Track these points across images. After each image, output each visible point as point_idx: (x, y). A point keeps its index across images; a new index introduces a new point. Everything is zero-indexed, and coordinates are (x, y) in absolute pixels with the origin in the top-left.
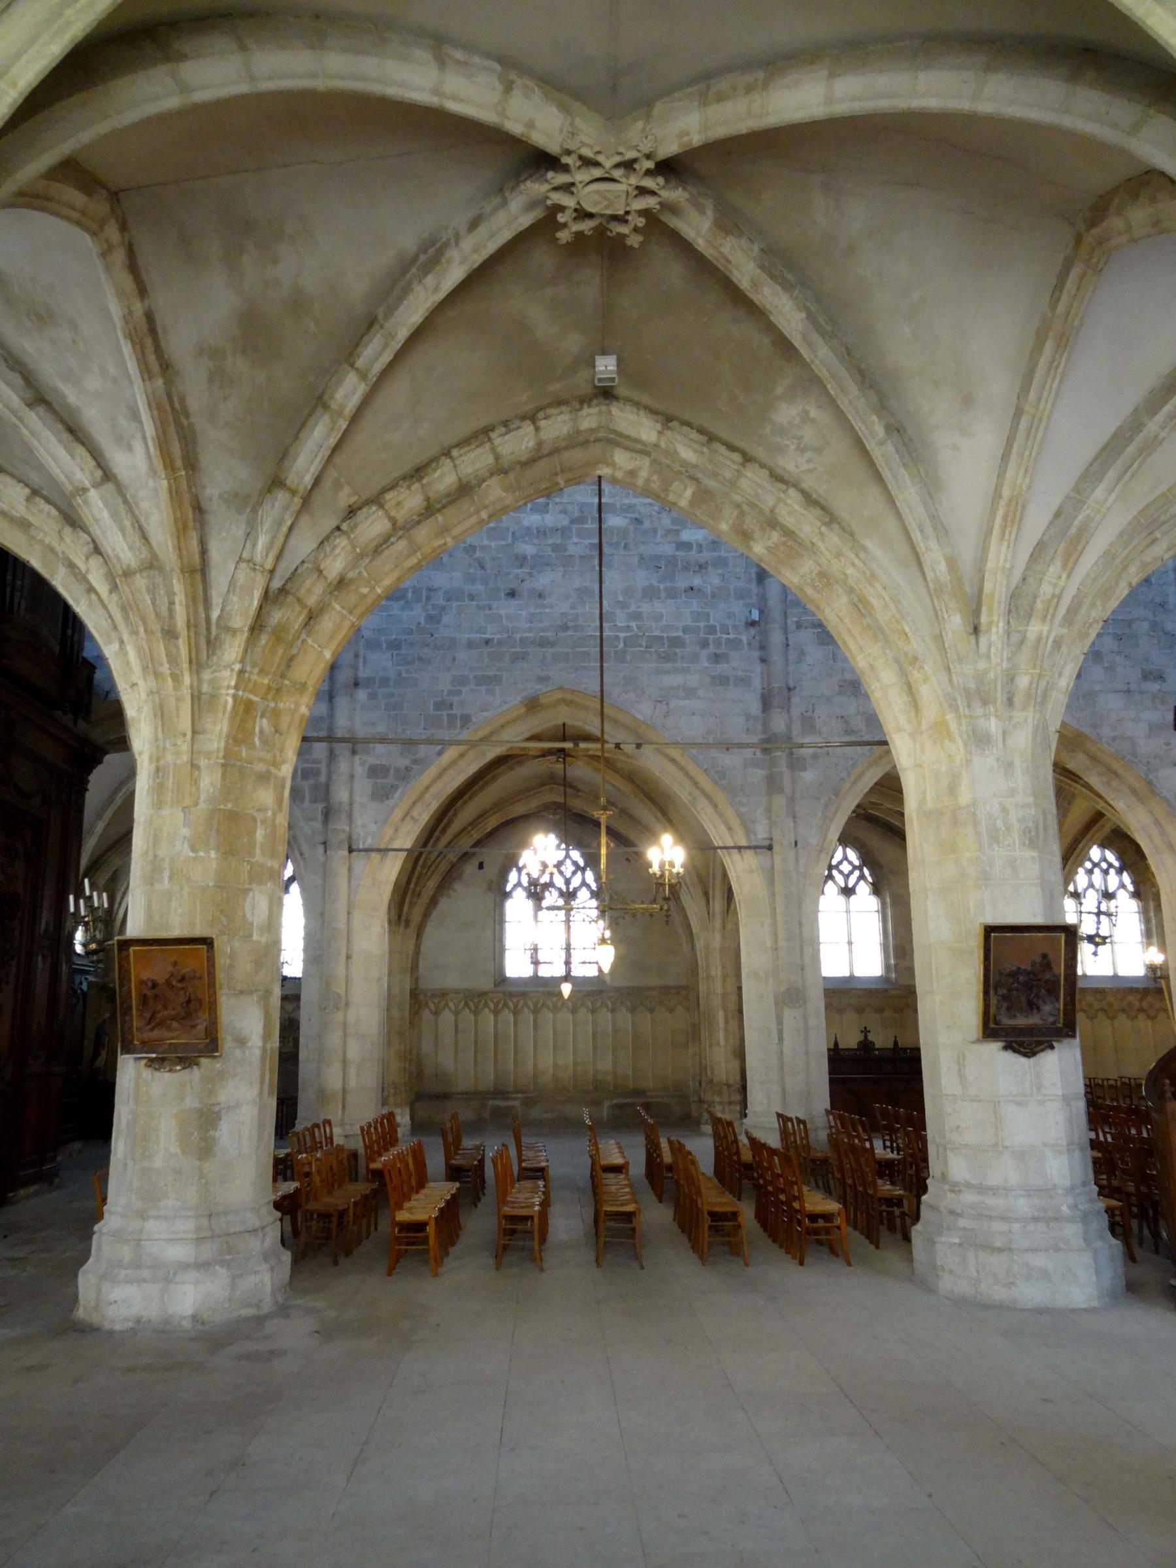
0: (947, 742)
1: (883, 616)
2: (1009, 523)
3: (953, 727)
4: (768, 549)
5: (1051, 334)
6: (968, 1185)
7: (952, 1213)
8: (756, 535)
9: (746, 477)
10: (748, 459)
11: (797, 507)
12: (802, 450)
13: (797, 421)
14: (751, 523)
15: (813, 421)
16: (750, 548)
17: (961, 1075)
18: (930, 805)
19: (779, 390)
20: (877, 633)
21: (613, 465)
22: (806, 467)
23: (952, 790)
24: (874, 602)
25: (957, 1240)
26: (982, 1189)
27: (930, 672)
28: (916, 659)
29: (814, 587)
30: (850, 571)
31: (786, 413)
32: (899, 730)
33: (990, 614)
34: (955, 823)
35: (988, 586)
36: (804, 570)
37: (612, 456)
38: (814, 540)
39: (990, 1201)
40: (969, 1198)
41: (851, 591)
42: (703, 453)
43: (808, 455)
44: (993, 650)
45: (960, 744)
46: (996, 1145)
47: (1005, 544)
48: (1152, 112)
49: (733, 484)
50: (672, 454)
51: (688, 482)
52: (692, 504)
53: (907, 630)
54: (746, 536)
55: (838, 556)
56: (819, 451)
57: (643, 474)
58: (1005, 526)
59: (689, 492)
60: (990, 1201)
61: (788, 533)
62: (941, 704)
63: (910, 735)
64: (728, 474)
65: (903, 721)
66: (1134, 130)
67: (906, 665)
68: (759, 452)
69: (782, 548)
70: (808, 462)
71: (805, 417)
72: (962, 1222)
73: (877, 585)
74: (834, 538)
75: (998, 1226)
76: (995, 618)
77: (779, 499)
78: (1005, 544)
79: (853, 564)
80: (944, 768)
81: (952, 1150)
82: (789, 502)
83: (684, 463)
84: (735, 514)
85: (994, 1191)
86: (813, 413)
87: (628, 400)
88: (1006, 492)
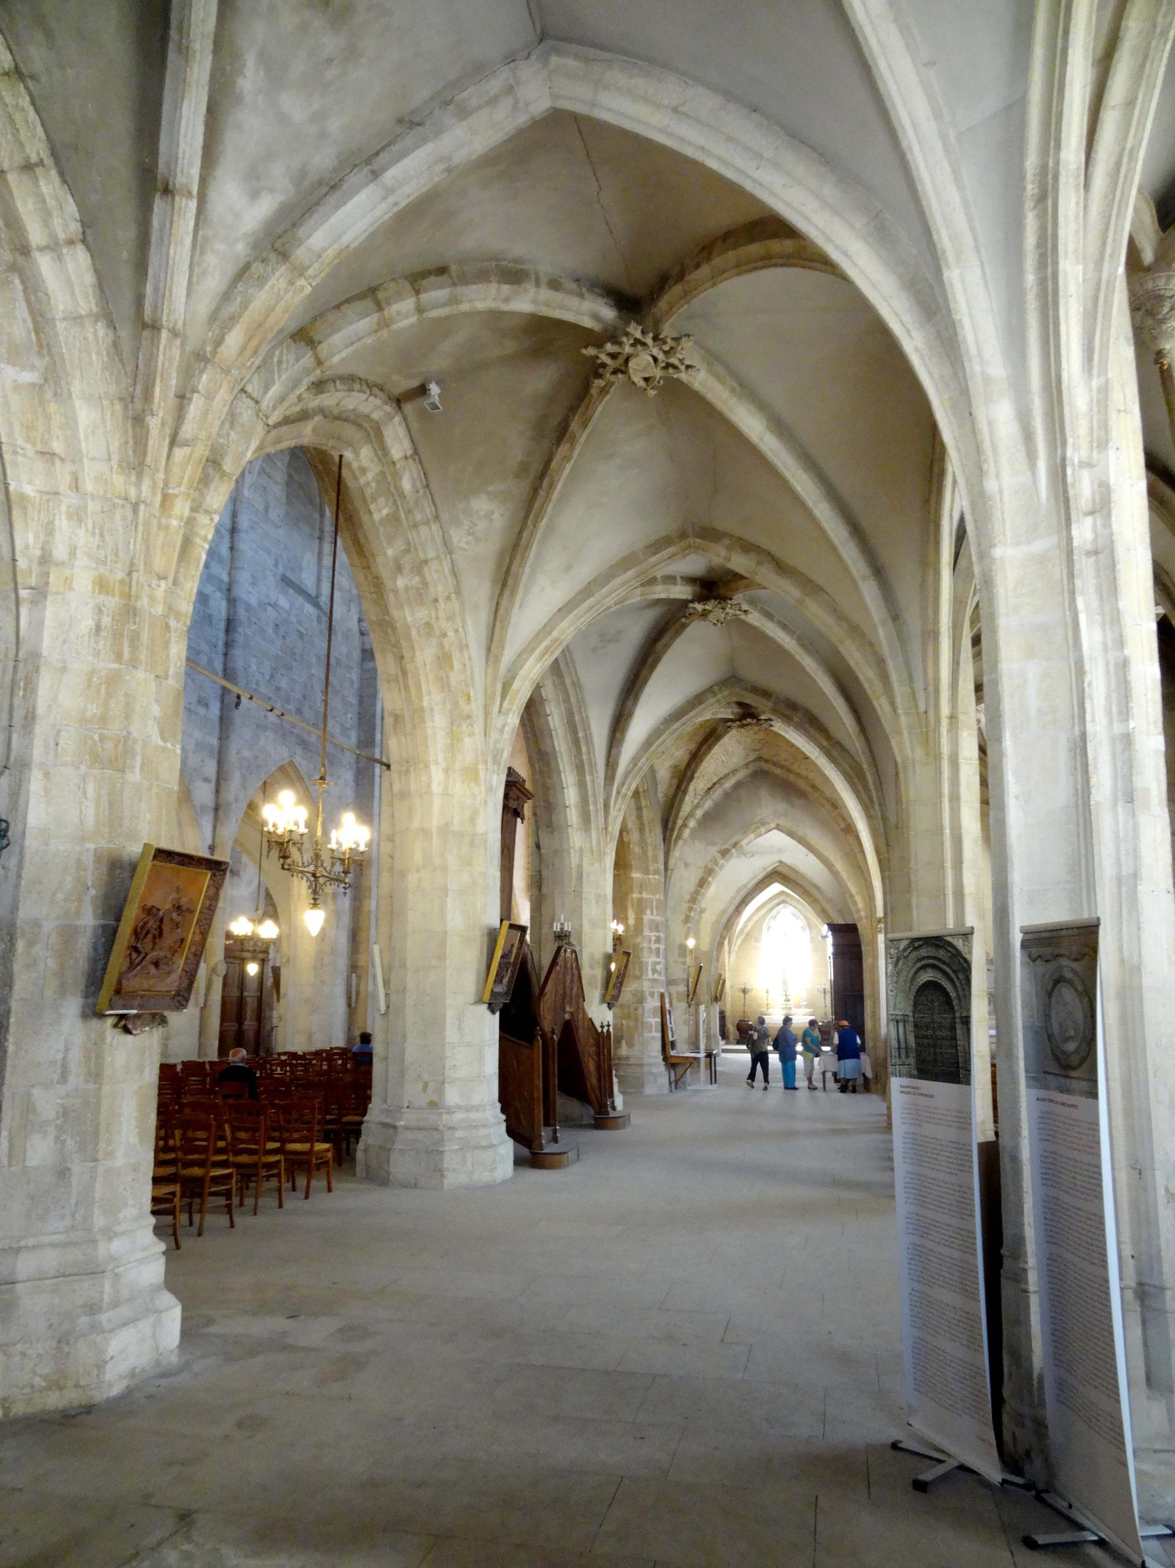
0: (472, 785)
1: (455, 677)
2: (549, 653)
3: (482, 775)
4: (406, 586)
5: (637, 568)
6: (459, 1107)
7: (450, 1128)
8: (405, 572)
9: (430, 528)
10: (437, 517)
11: (446, 570)
12: (469, 533)
13: (482, 514)
14: (407, 561)
15: (491, 520)
16: (395, 580)
17: (460, 1028)
18: (456, 826)
19: (491, 488)
20: (445, 685)
21: (357, 454)
22: (463, 545)
23: (473, 819)
24: (456, 665)
25: (456, 1147)
26: (468, 1109)
27: (477, 731)
28: (469, 717)
29: (419, 632)
30: (451, 634)
31: (481, 504)
32: (437, 763)
33: (511, 703)
34: (472, 845)
35: (516, 685)
36: (418, 615)
37: (361, 447)
38: (440, 600)
39: (474, 1116)
40: (459, 1116)
41: (441, 646)
42: (418, 492)
43: (470, 538)
44: (506, 728)
45: (483, 789)
46: (479, 1076)
47: (540, 664)
48: (872, 578)
49: (415, 526)
50: (397, 476)
51: (390, 504)
52: (382, 520)
53: (472, 695)
54: (399, 569)
55: (450, 618)
56: (478, 540)
57: (370, 476)
58: (545, 654)
59: (385, 512)
60: (474, 1116)
61: (425, 583)
62: (477, 756)
63: (443, 770)
64: (419, 517)
65: (441, 758)
66: (864, 578)
67: (458, 718)
68: (445, 516)
69: (414, 591)
70: (467, 543)
71: (488, 516)
72: (458, 1134)
73: (465, 653)
74: (456, 605)
75: (483, 1132)
76: (514, 708)
77: (438, 557)
78: (540, 664)
79: (457, 631)
80: (468, 802)
81: (449, 1083)
82: (444, 564)
83: (398, 488)
84: (403, 548)
85: (477, 1108)
86: (496, 516)
87: (405, 419)
88: (555, 633)
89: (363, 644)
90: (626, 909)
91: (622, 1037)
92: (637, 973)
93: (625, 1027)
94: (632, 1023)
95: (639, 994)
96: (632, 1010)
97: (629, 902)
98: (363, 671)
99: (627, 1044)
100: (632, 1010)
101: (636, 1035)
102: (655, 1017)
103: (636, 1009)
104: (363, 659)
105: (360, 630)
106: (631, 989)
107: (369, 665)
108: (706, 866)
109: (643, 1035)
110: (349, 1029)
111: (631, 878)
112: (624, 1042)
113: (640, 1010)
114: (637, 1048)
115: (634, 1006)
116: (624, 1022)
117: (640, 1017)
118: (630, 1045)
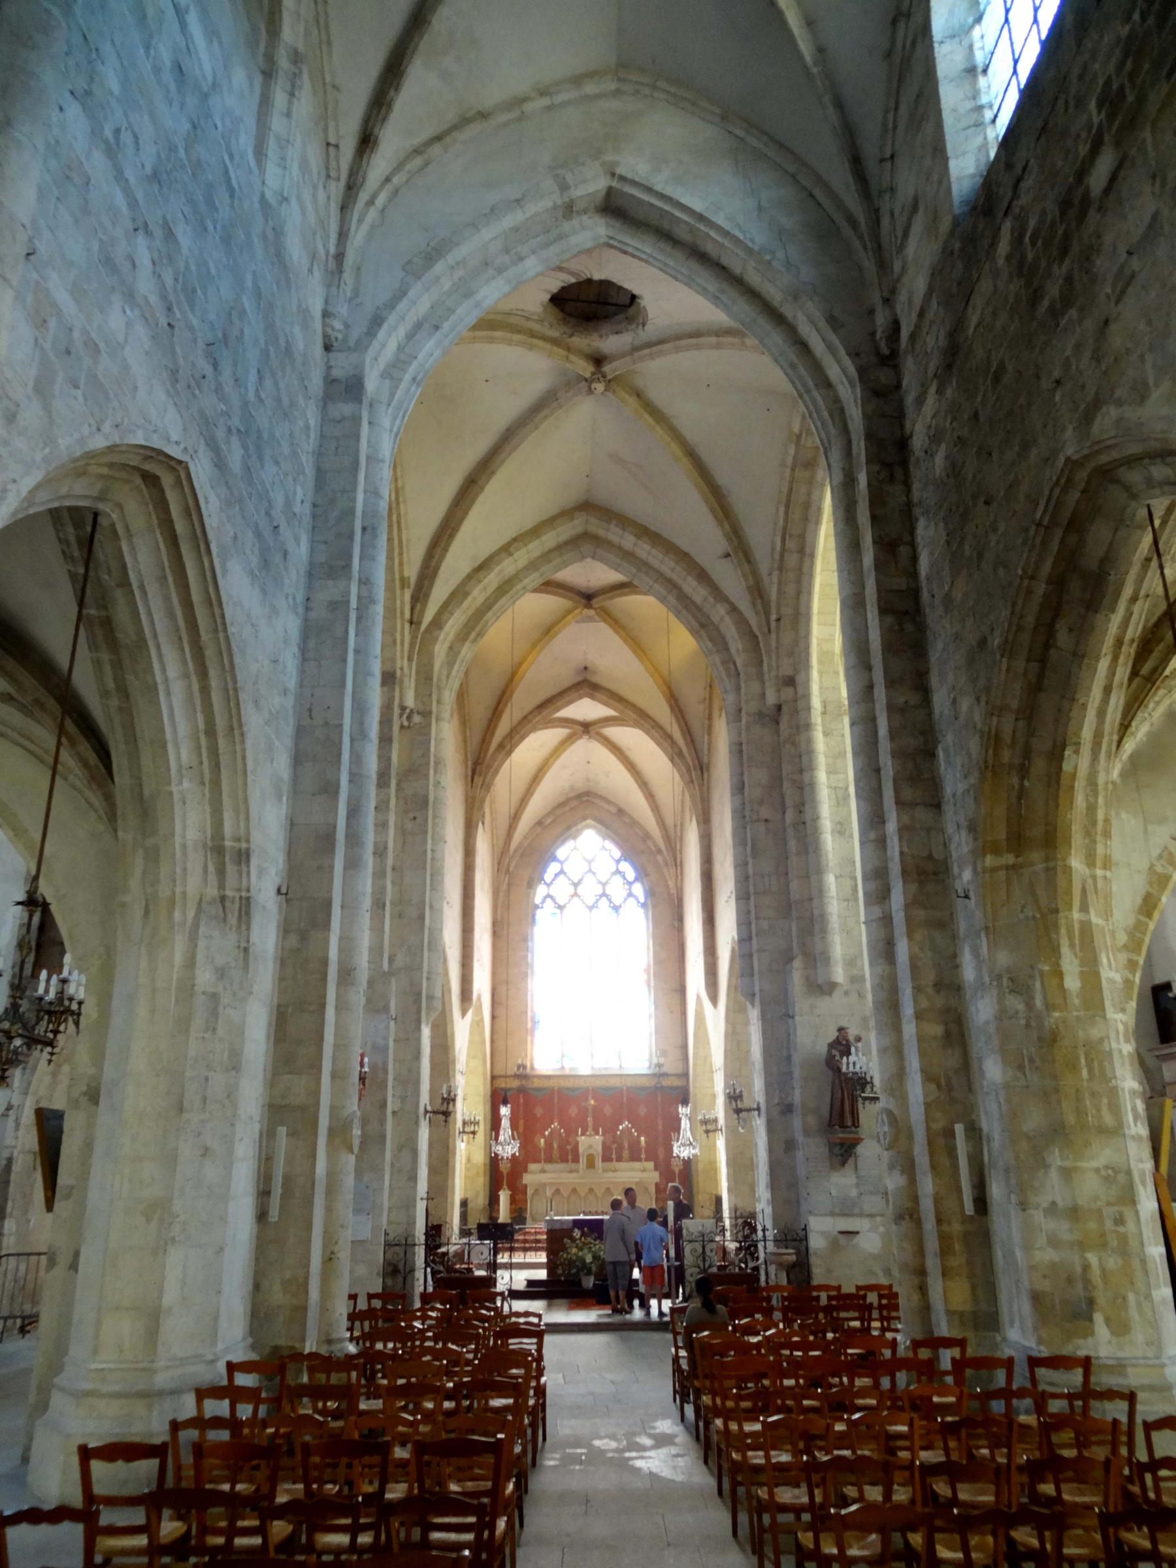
89: (329, 368)
90: (1056, 951)
91: (1091, 1302)
92: (1108, 1120)
93: (1096, 1271)
94: (1113, 1262)
95: (1121, 1178)
96: (1109, 1224)
97: (1063, 931)
98: (325, 419)
99: (1108, 1321)
100: (1109, 1224)
101: (1131, 1297)
102: (1156, 1245)
103: (1120, 1221)
104: (327, 399)
105: (326, 336)
106: (1095, 1164)
107: (347, 409)
108: (1151, 867)
109: (1148, 1297)
110: (257, 1287)
111: (1068, 870)
112: (1098, 1318)
113: (1131, 1226)
114: (1139, 1336)
115: (1108, 1212)
116: (1093, 1258)
117: (1133, 1243)
118: (1120, 1328)
